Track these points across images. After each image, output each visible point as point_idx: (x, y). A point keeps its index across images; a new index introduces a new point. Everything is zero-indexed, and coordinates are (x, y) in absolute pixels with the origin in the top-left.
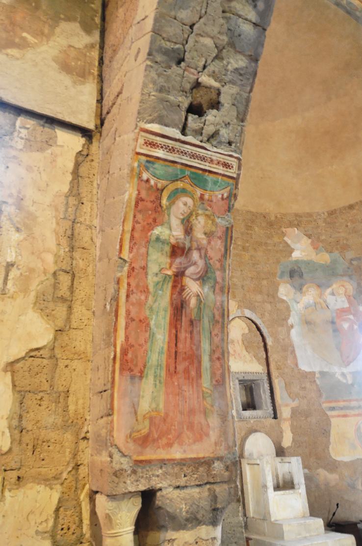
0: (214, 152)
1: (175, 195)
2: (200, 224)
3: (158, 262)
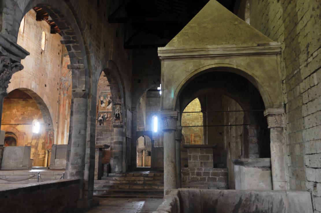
0: (51, 127)
1: (49, 131)
2: (51, 133)
3: (48, 136)
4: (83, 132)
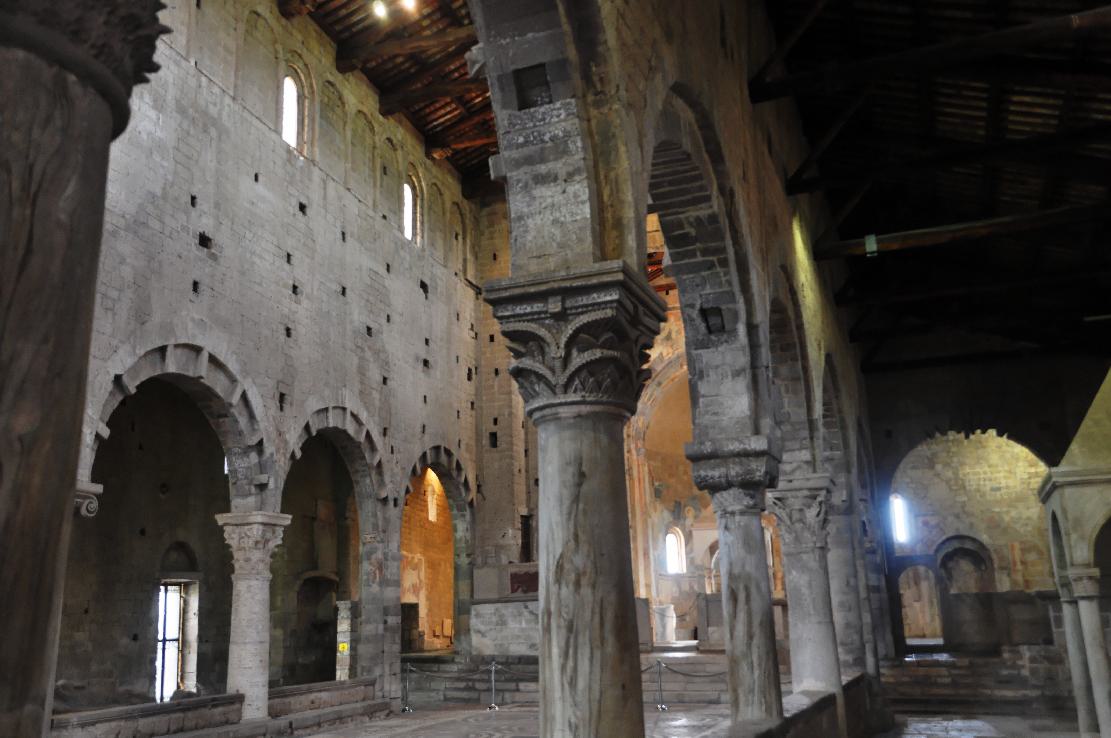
4: (852, 581)
